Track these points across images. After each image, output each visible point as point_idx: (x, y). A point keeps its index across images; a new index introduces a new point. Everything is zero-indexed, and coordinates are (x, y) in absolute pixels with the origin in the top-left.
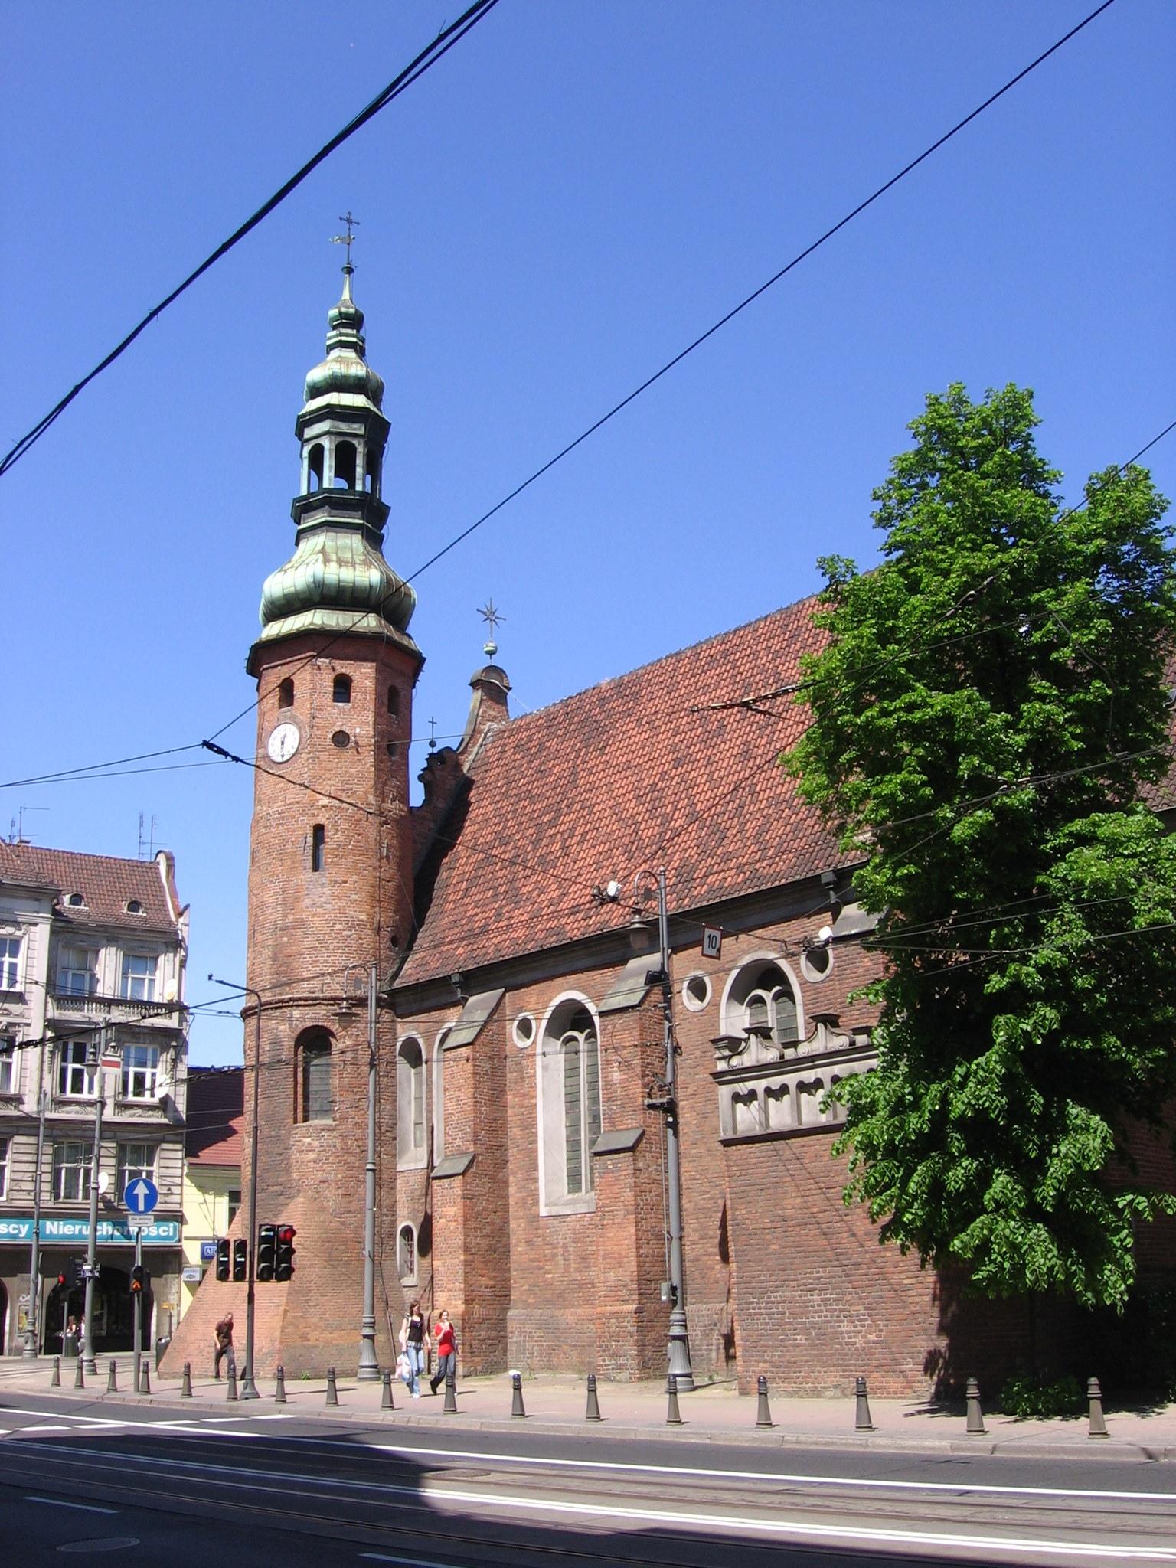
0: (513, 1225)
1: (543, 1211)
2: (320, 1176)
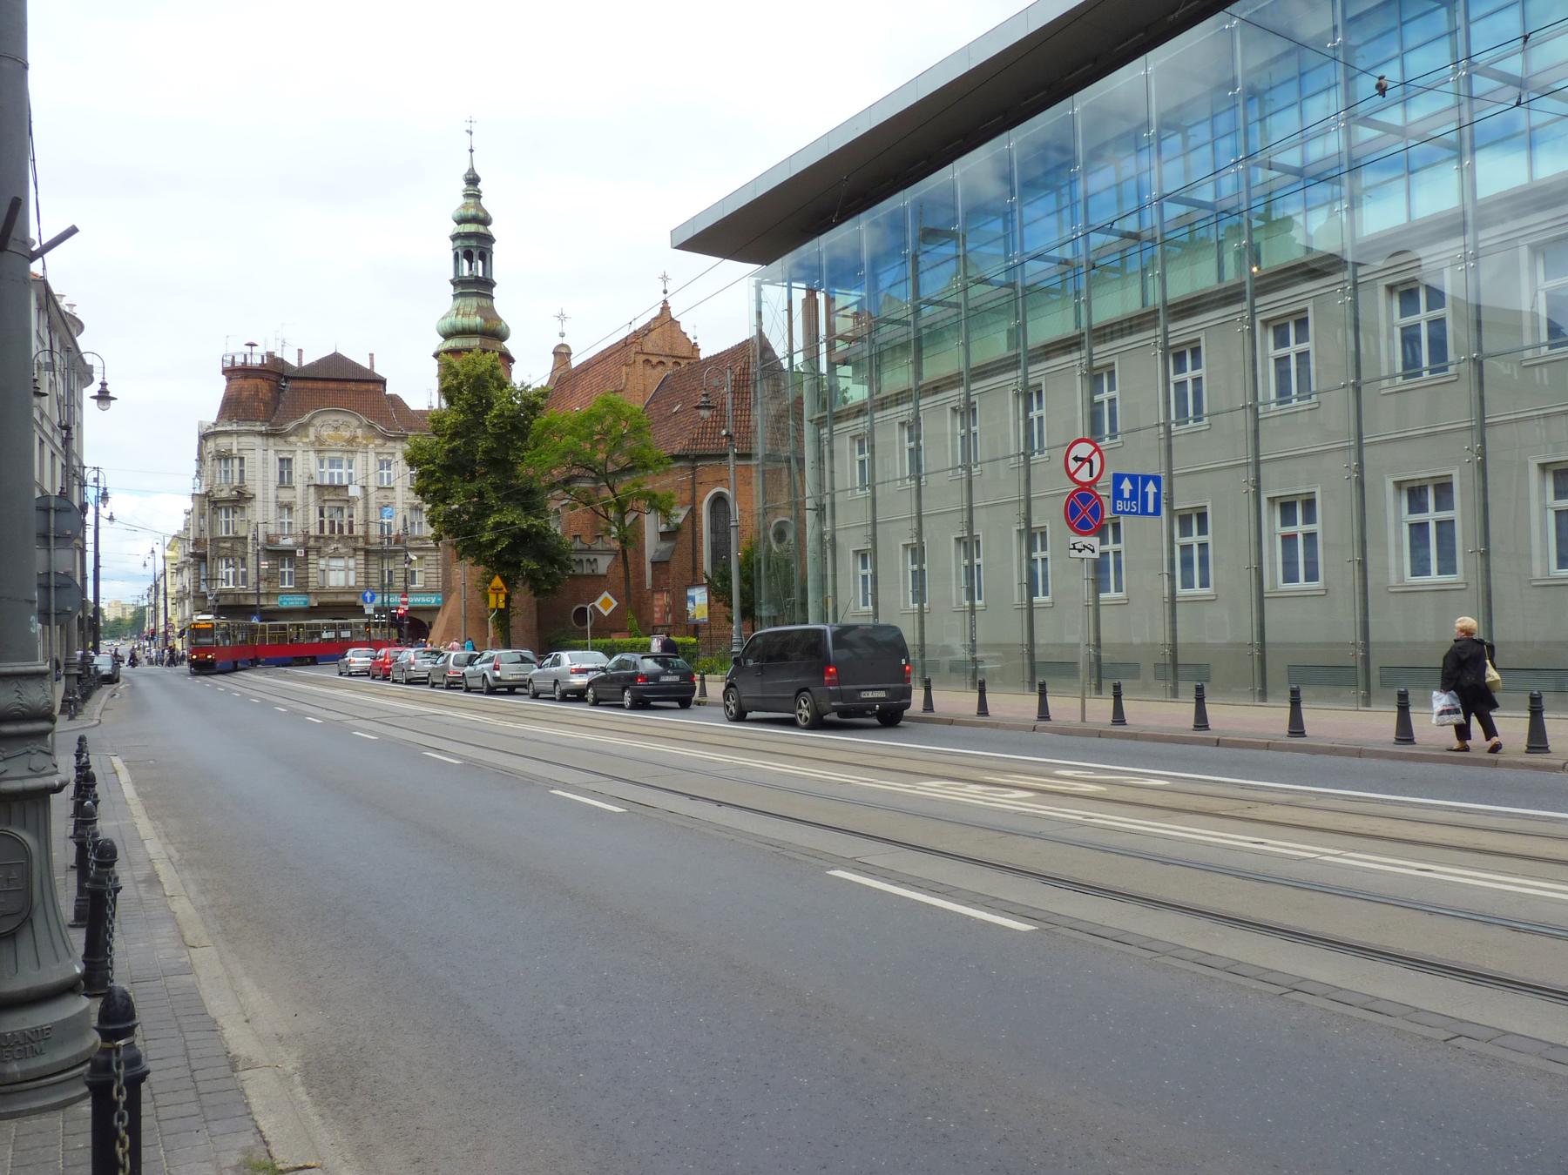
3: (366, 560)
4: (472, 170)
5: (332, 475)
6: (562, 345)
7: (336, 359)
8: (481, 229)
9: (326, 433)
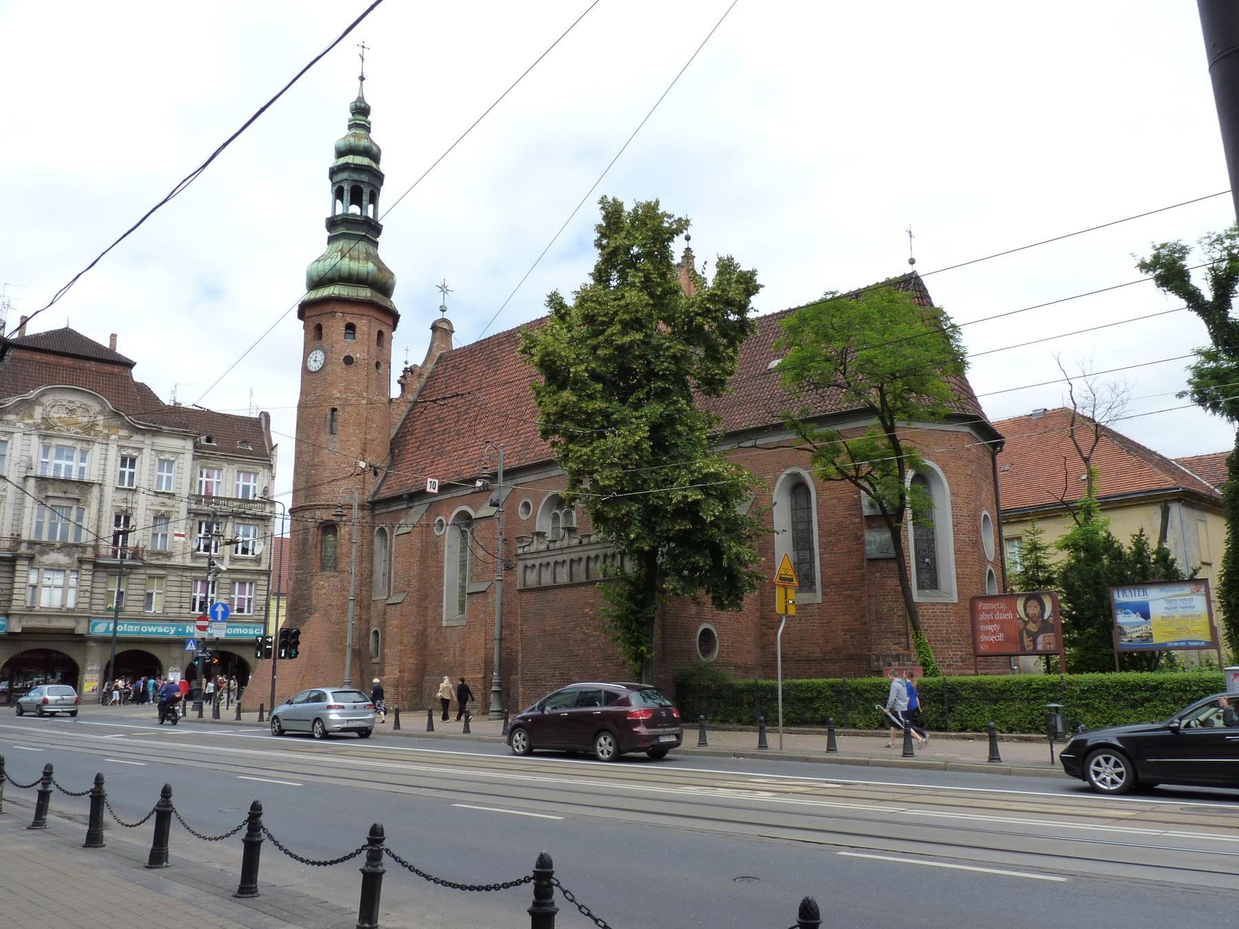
0: (429, 630)
1: (444, 624)
2: (328, 602)
3: (93, 575)
4: (361, 99)
5: (57, 467)
6: (444, 320)
7: (67, 334)
8: (374, 165)
9: (56, 414)
